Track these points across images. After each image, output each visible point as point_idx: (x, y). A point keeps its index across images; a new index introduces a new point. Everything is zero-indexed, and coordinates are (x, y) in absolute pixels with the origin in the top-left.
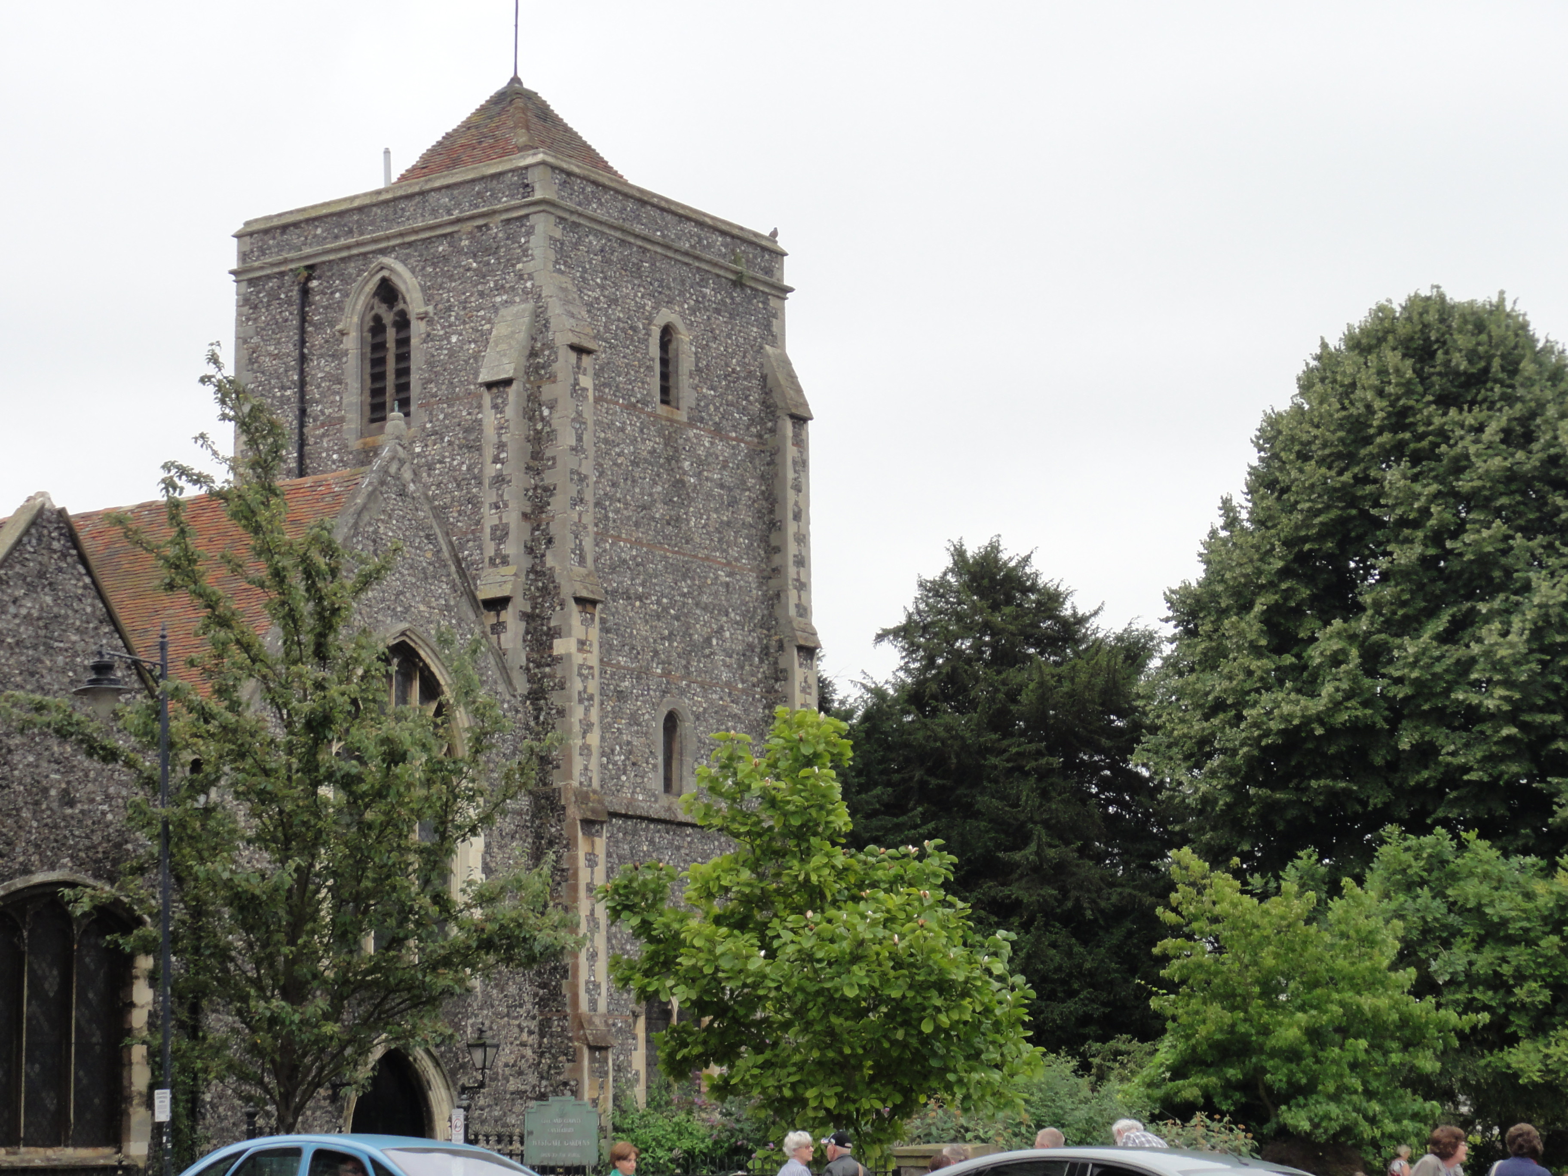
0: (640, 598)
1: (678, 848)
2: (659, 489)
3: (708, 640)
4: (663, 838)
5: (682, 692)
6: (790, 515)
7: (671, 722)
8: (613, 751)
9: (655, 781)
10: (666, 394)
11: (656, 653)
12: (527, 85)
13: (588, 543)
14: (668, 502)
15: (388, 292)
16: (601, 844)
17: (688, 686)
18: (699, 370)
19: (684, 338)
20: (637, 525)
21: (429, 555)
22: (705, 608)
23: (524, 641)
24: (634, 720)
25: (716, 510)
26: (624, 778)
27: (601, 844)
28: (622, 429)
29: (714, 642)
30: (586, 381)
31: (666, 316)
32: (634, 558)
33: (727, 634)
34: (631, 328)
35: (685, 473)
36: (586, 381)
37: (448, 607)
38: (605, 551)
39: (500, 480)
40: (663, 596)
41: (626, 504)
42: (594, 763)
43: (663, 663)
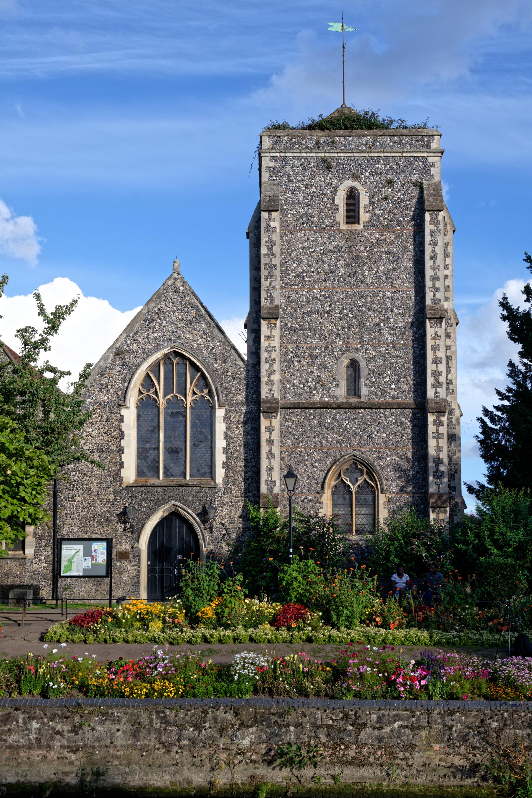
0: (328, 312)
1: (353, 420)
2: (341, 262)
3: (378, 325)
5: (357, 350)
7: (354, 365)
8: (307, 381)
10: (352, 217)
11: (338, 335)
14: (347, 265)
17: (362, 347)
18: (372, 204)
20: (325, 281)
21: (194, 315)
22: (376, 310)
23: (254, 341)
25: (384, 265)
26: (315, 392)
28: (316, 240)
29: (382, 325)
31: (348, 183)
32: (323, 296)
33: (392, 320)
34: (322, 194)
35: (360, 252)
37: (205, 333)
38: (303, 295)
40: (343, 309)
41: (318, 273)
43: (344, 338)
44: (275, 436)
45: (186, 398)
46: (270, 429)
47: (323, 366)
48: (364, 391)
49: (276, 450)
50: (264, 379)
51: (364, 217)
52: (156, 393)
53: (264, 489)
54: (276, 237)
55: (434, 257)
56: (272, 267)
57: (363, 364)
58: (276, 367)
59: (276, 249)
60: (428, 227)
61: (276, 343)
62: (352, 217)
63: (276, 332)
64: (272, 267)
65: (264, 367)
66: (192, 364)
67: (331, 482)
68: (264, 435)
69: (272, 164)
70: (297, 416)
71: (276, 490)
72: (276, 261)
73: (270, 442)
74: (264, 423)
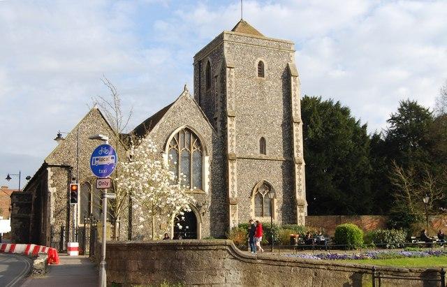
3: (272, 123)
4: (259, 162)
6: (293, 96)
7: (263, 140)
9: (258, 151)
10: (261, 73)
12: (244, 20)
13: (233, 105)
15: (209, 62)
16: (235, 165)
19: (265, 63)
24: (251, 139)
27: (235, 165)
30: (233, 74)
31: (259, 59)
36: (233, 74)
39: (217, 95)
42: (234, 148)
44: (235, 171)
45: (190, 150)
46: (233, 167)
47: (251, 139)
48: (267, 152)
49: (235, 178)
50: (229, 144)
51: (266, 74)
52: (177, 147)
53: (230, 196)
54: (233, 80)
55: (295, 96)
56: (231, 93)
57: (267, 139)
58: (234, 139)
59: (233, 85)
60: (293, 83)
61: (234, 128)
62: (261, 73)
63: (234, 123)
64: (231, 93)
65: (229, 139)
66: (195, 136)
67: (254, 193)
68: (230, 170)
69: (228, 46)
70: (241, 161)
71: (236, 196)
72: (233, 90)
73: (233, 173)
74: (230, 165)
